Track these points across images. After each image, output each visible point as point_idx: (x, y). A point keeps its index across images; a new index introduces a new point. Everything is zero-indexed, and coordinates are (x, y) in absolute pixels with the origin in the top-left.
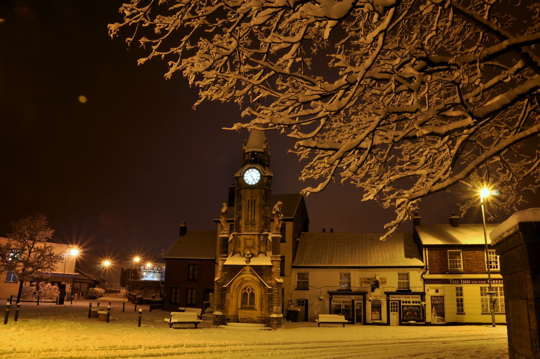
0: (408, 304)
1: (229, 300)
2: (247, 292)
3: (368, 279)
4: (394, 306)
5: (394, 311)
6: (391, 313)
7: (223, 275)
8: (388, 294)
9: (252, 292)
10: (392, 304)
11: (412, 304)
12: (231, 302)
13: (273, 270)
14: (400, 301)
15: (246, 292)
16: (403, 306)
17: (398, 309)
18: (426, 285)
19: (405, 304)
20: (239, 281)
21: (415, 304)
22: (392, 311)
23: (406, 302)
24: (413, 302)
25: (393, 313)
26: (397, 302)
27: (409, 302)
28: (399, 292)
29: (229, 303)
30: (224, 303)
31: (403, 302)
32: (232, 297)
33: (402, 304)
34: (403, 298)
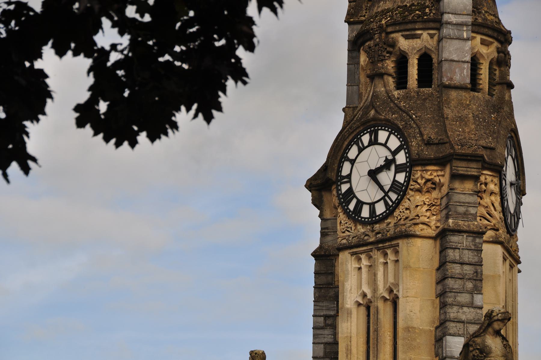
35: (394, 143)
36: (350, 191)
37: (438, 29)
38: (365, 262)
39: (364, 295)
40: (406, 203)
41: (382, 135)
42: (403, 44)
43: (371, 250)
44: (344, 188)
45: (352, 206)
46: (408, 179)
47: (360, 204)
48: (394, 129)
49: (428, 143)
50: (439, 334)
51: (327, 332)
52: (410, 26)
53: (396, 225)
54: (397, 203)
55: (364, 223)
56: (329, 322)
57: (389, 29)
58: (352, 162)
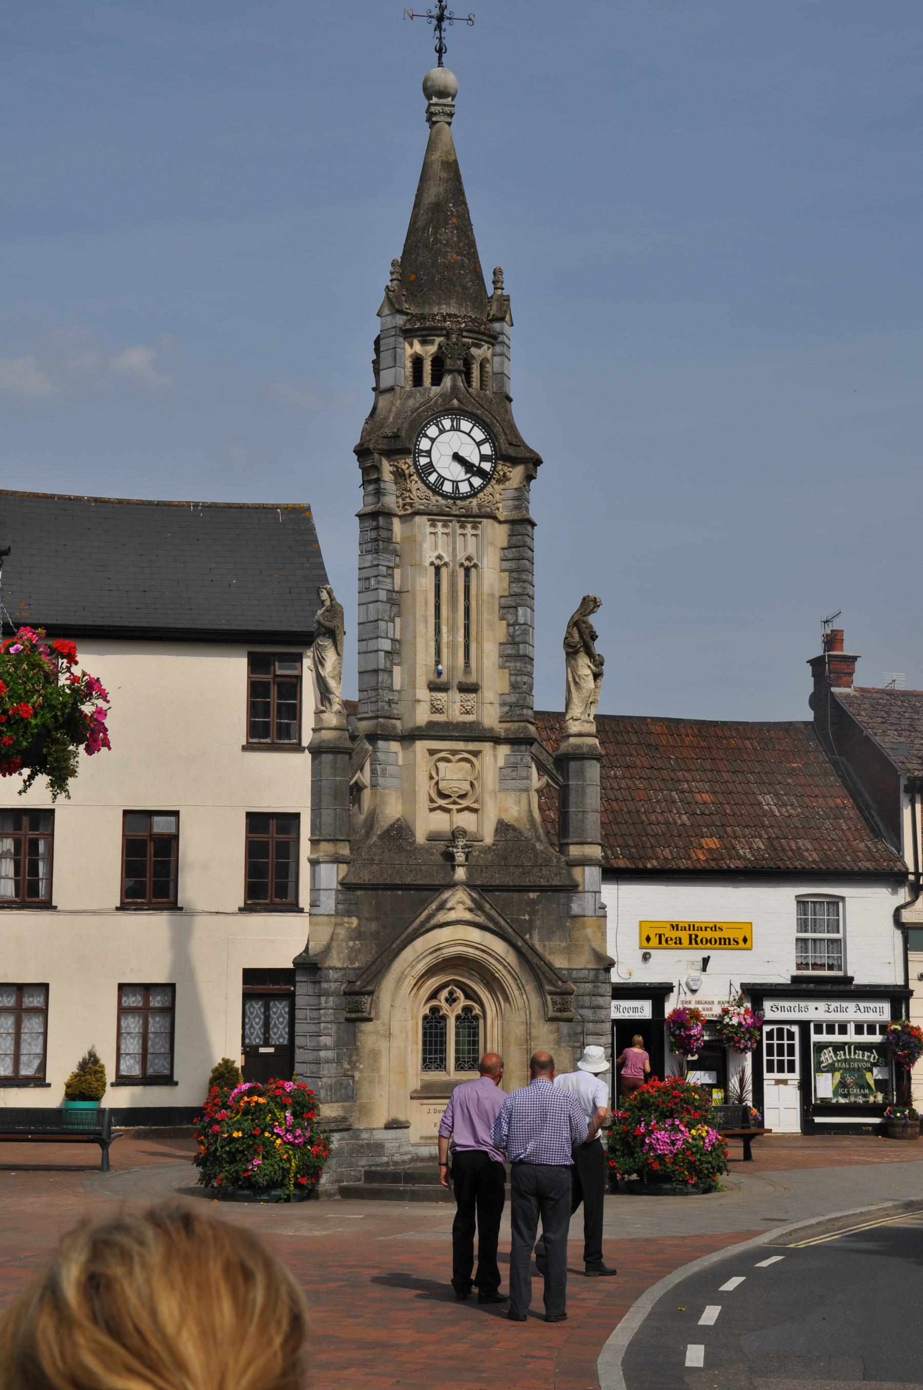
0: (837, 1038)
1: (375, 1055)
2: (445, 1008)
3: (675, 927)
4: (436, 1036)
5: (781, 1070)
6: (766, 1075)
7: (342, 932)
8: (756, 994)
9: (467, 1009)
10: (770, 1035)
11: (851, 1037)
12: (384, 1062)
13: (575, 908)
14: (804, 1025)
15: (435, 1010)
16: (820, 1047)
17: (797, 1058)
18: (912, 956)
19: (824, 1038)
20: (418, 960)
21: (866, 1038)
22: (770, 1070)
23: (831, 1030)
24: (859, 1030)
25: (777, 1076)
26: (795, 1029)
27: (843, 1030)
28: (800, 989)
29: (375, 1069)
30: (354, 1067)
31: (818, 1030)
32: (389, 1035)
33: (815, 1038)
34: (816, 1011)
35: (479, 434)
36: (430, 465)
37: (493, 345)
38: (440, 528)
39: (439, 557)
40: (489, 489)
41: (466, 425)
42: (473, 350)
43: (451, 521)
44: (423, 461)
45: (432, 478)
46: (494, 468)
47: (442, 479)
48: (478, 421)
49: (510, 444)
50: (510, 602)
51: (388, 580)
52: (480, 337)
53: (480, 506)
54: (482, 488)
55: (445, 496)
56: (390, 572)
57: (465, 334)
58: (433, 440)
